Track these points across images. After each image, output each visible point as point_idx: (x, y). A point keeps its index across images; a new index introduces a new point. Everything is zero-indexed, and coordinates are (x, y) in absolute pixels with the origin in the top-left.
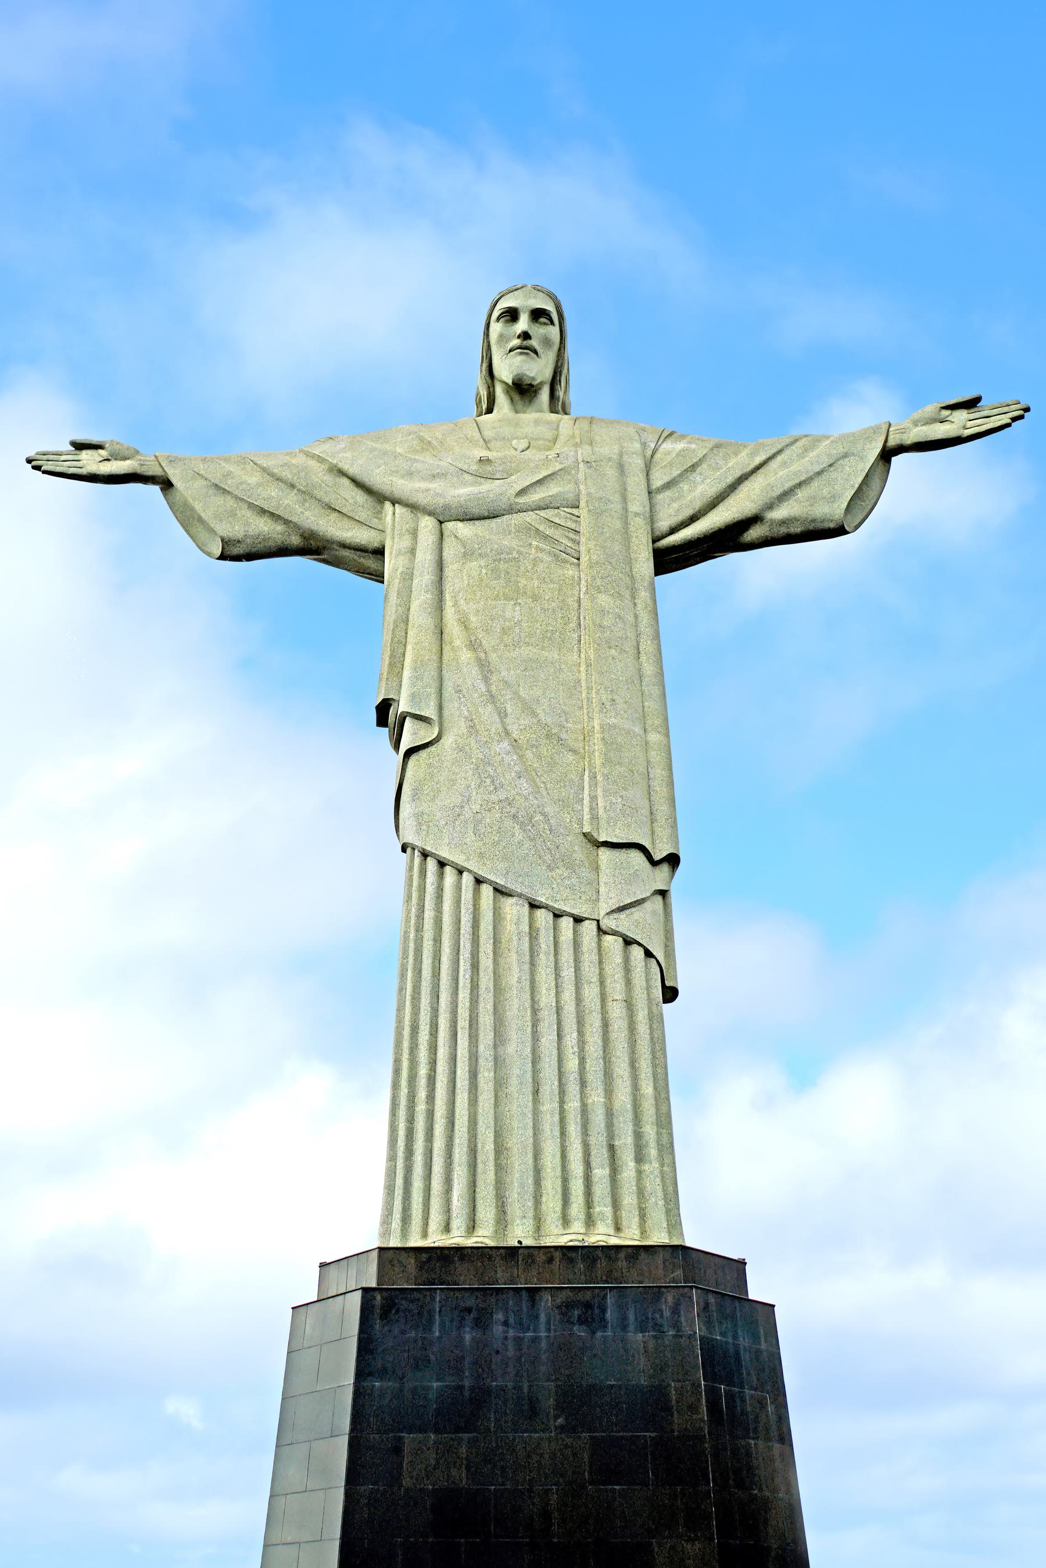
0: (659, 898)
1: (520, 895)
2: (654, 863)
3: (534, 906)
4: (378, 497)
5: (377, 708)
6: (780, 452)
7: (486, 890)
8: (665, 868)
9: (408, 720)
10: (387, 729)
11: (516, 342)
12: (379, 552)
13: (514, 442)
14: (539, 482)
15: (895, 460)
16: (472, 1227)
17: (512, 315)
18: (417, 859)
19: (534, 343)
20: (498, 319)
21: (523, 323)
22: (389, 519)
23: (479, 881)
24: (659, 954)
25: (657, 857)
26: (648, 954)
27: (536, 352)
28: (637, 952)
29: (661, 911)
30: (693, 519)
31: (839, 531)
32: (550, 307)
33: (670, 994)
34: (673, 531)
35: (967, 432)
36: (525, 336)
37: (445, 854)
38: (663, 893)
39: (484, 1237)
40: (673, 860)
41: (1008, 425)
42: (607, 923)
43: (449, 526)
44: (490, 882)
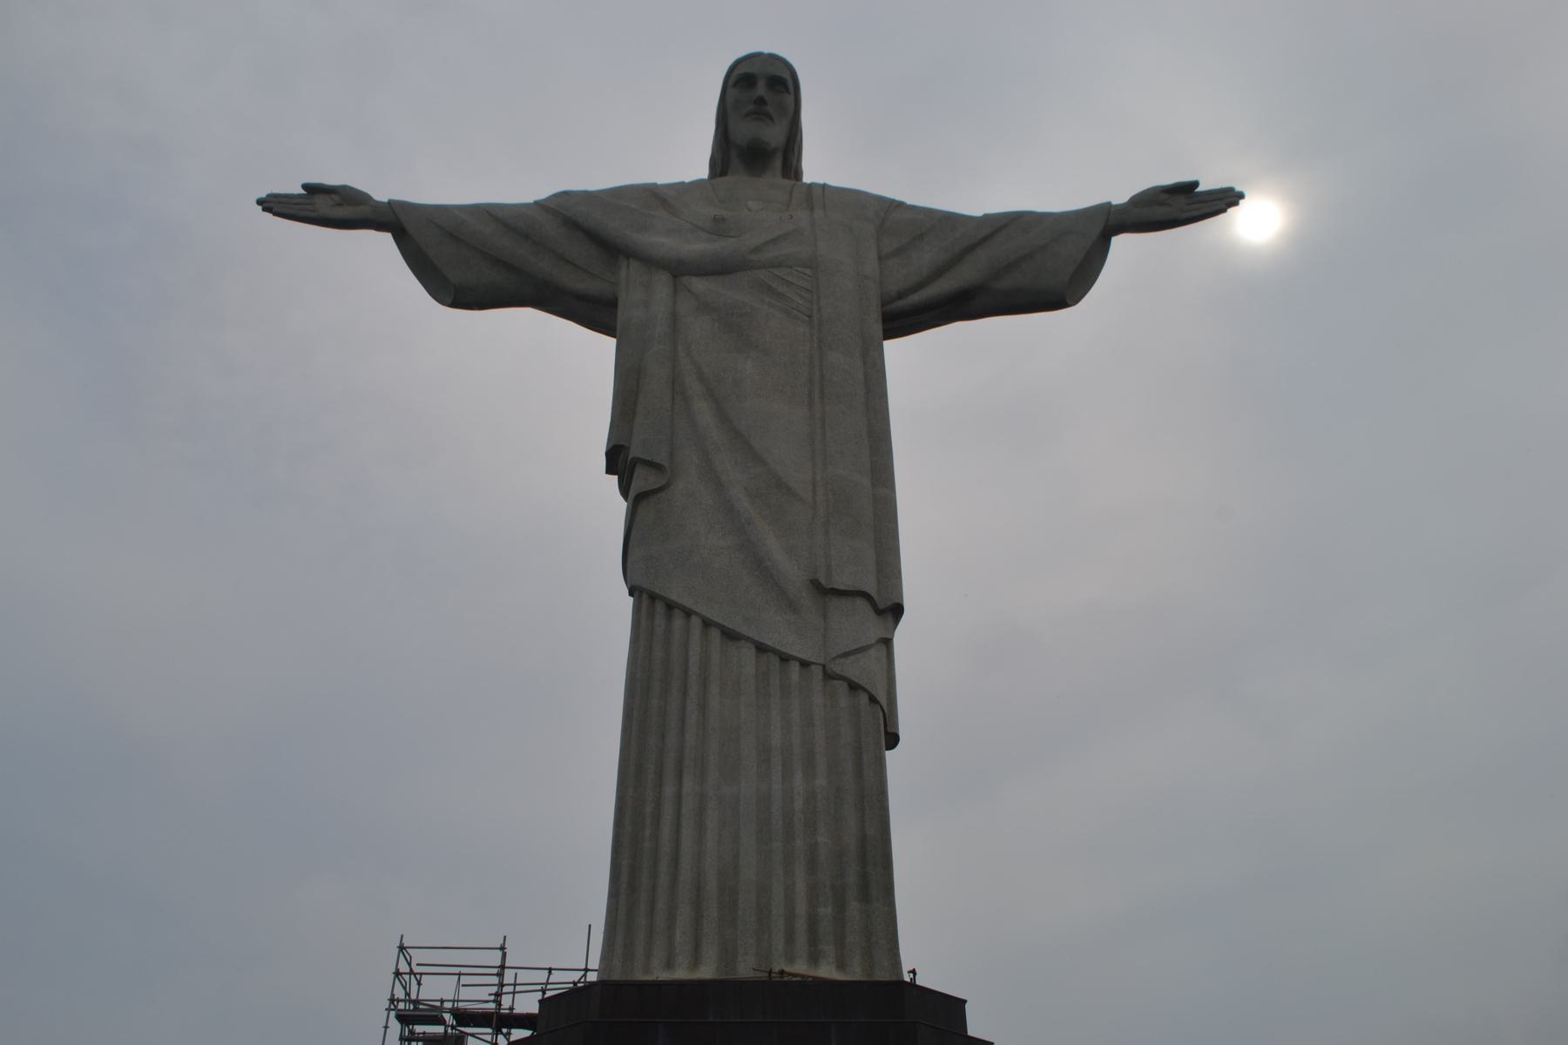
0: (884, 648)
1: (748, 639)
2: (879, 612)
3: (761, 648)
4: (613, 251)
5: (608, 454)
6: (1005, 226)
7: (715, 634)
8: (890, 619)
10: (615, 478)
11: (751, 107)
12: (612, 304)
13: (750, 204)
14: (774, 241)
15: (1114, 239)
16: (696, 962)
18: (645, 602)
19: (769, 109)
20: (735, 85)
21: (761, 90)
22: (623, 273)
23: (707, 624)
24: (884, 702)
25: (881, 606)
27: (771, 119)
28: (864, 699)
29: (884, 660)
30: (920, 286)
32: (786, 75)
33: (892, 740)
35: (1184, 216)
36: (761, 101)
37: (674, 596)
38: (887, 643)
39: (706, 972)
40: (897, 611)
41: (1224, 211)
42: (836, 668)
43: (685, 279)
44: (717, 625)
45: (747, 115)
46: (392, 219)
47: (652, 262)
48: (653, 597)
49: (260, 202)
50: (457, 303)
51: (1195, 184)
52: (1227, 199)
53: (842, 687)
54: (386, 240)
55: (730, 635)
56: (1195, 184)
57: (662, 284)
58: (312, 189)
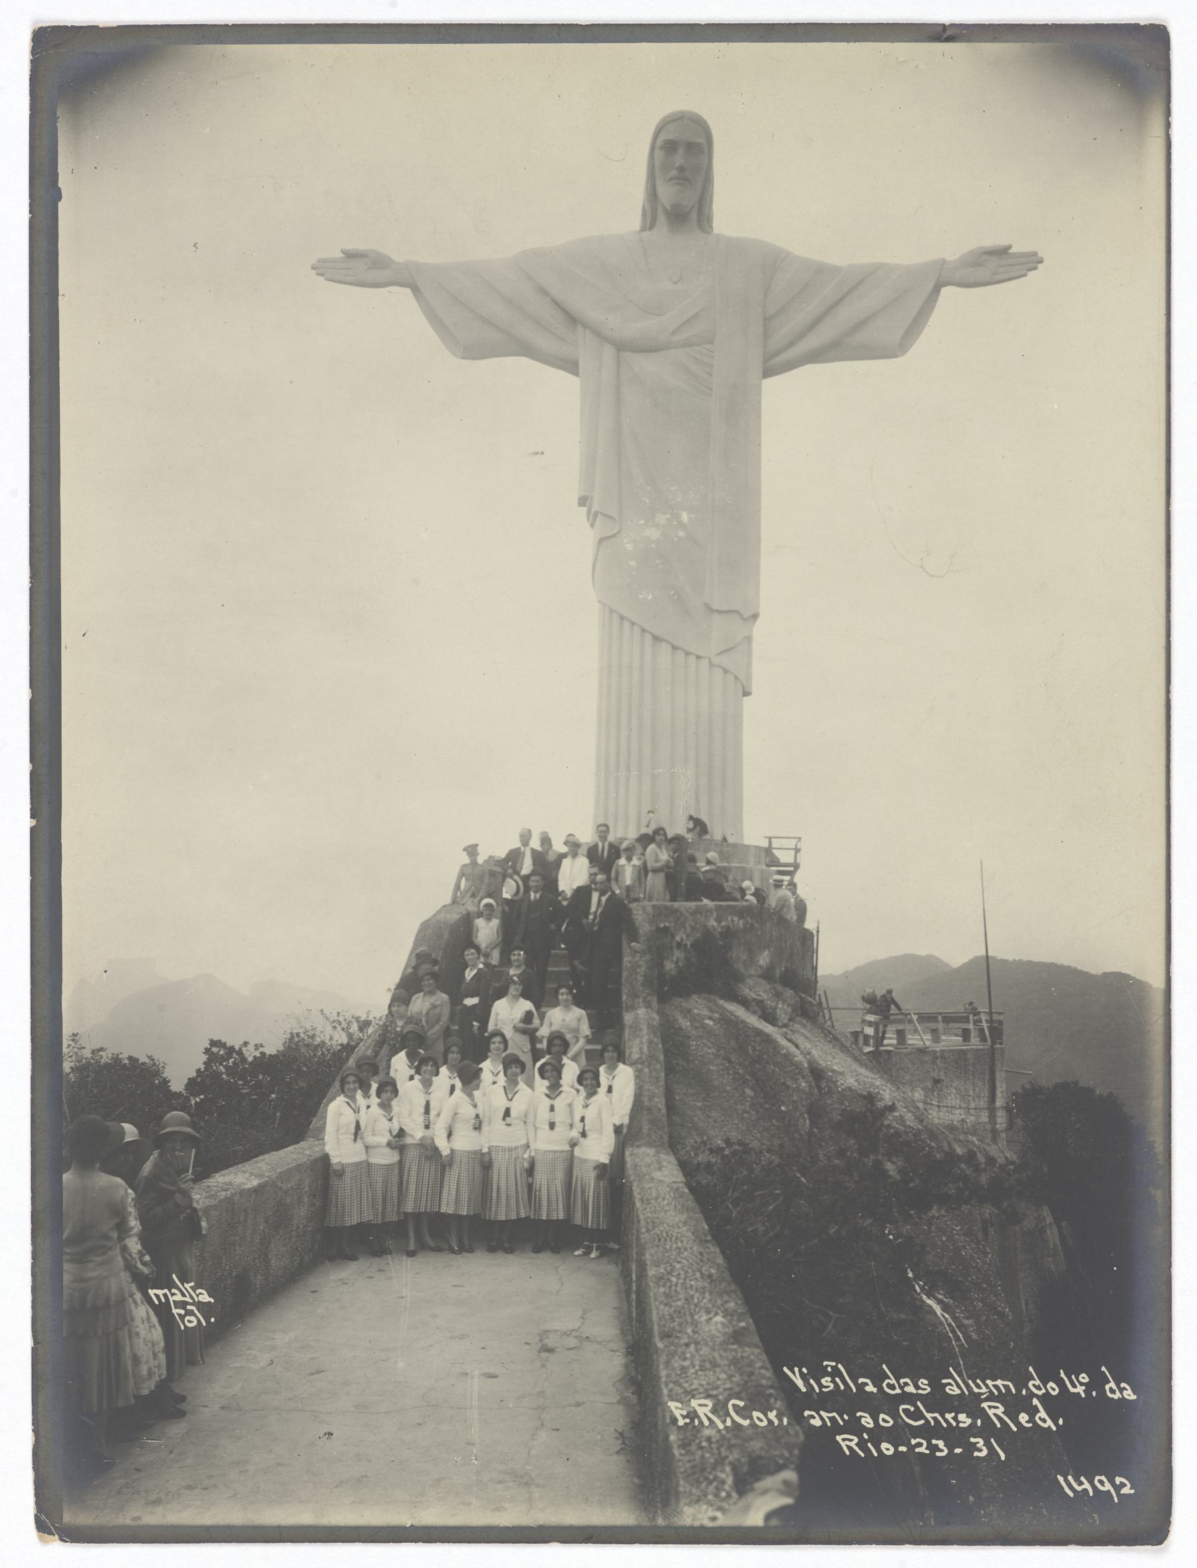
1: (667, 642)
3: (674, 648)
4: (572, 319)
9: (599, 517)
10: (585, 509)
11: (674, 173)
17: (670, 147)
20: (661, 148)
23: (643, 631)
25: (747, 614)
26: (736, 678)
31: (894, 356)
34: (778, 353)
36: (681, 169)
38: (749, 639)
40: (755, 616)
41: (1025, 275)
42: (716, 660)
45: (671, 179)
46: (409, 279)
47: (600, 336)
48: (612, 611)
49: (313, 268)
50: (463, 358)
51: (1010, 247)
52: (1032, 261)
53: (718, 673)
54: (408, 290)
55: (656, 639)
56: (1010, 247)
57: (608, 353)
58: (350, 255)
